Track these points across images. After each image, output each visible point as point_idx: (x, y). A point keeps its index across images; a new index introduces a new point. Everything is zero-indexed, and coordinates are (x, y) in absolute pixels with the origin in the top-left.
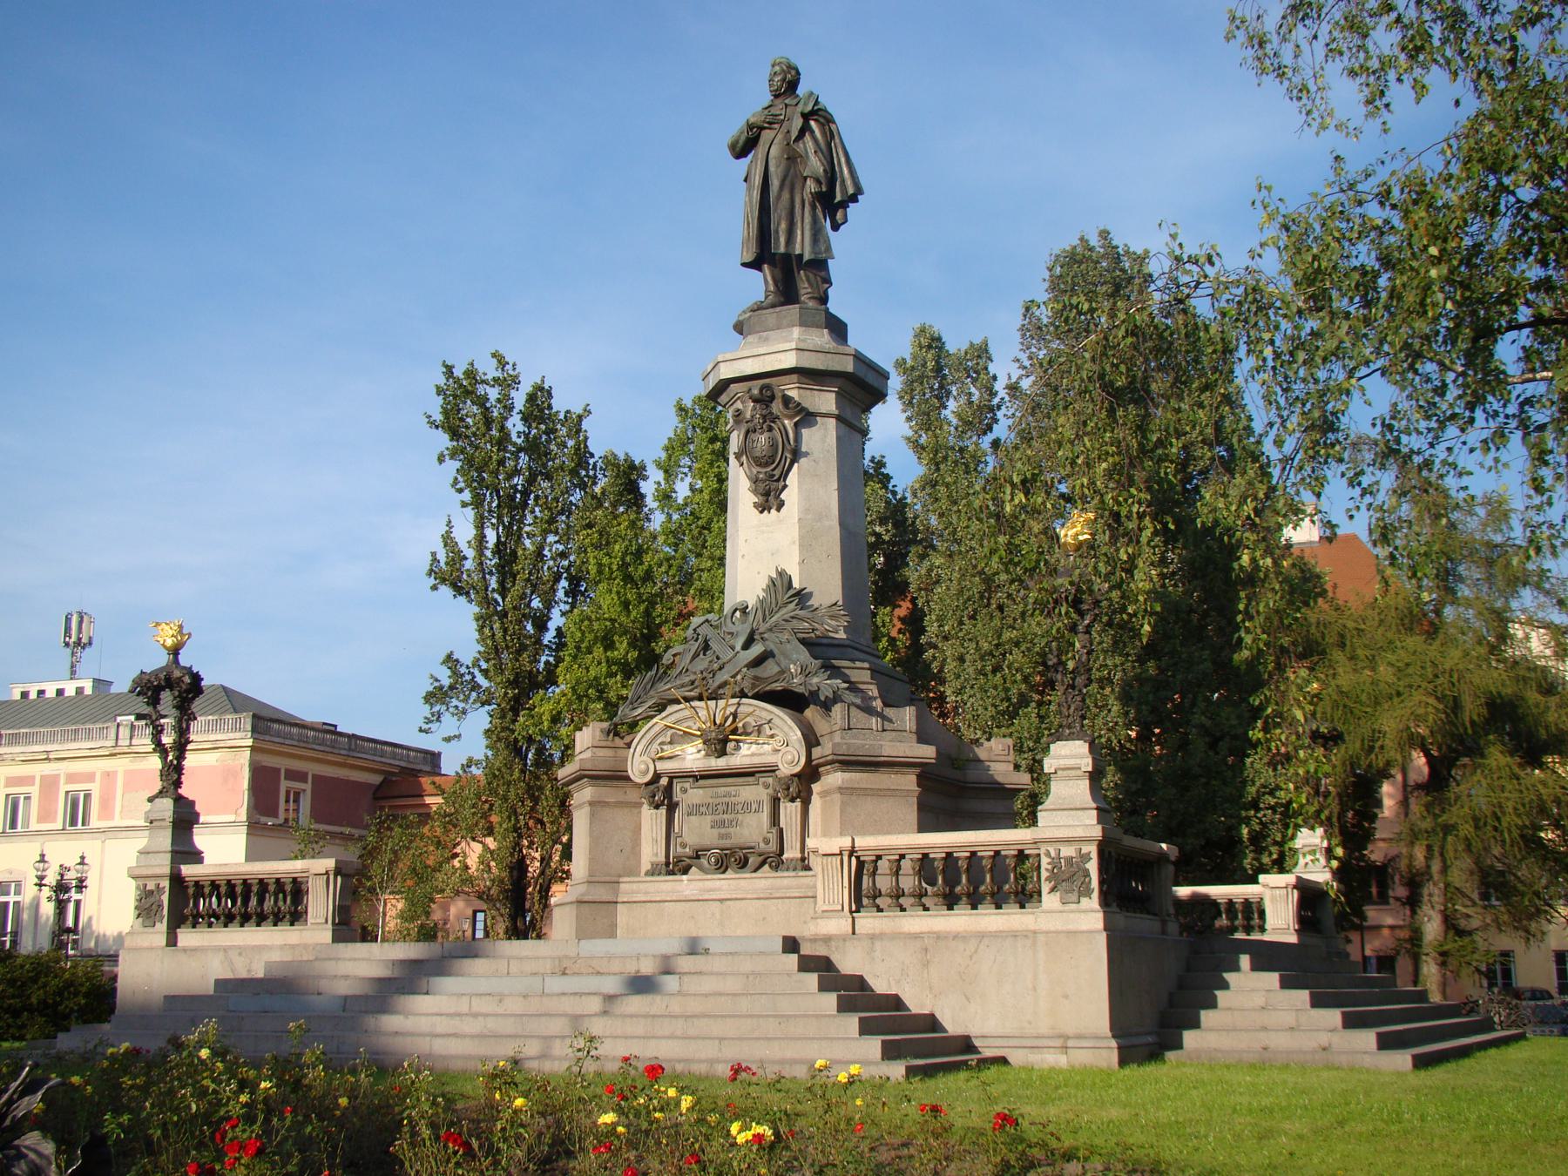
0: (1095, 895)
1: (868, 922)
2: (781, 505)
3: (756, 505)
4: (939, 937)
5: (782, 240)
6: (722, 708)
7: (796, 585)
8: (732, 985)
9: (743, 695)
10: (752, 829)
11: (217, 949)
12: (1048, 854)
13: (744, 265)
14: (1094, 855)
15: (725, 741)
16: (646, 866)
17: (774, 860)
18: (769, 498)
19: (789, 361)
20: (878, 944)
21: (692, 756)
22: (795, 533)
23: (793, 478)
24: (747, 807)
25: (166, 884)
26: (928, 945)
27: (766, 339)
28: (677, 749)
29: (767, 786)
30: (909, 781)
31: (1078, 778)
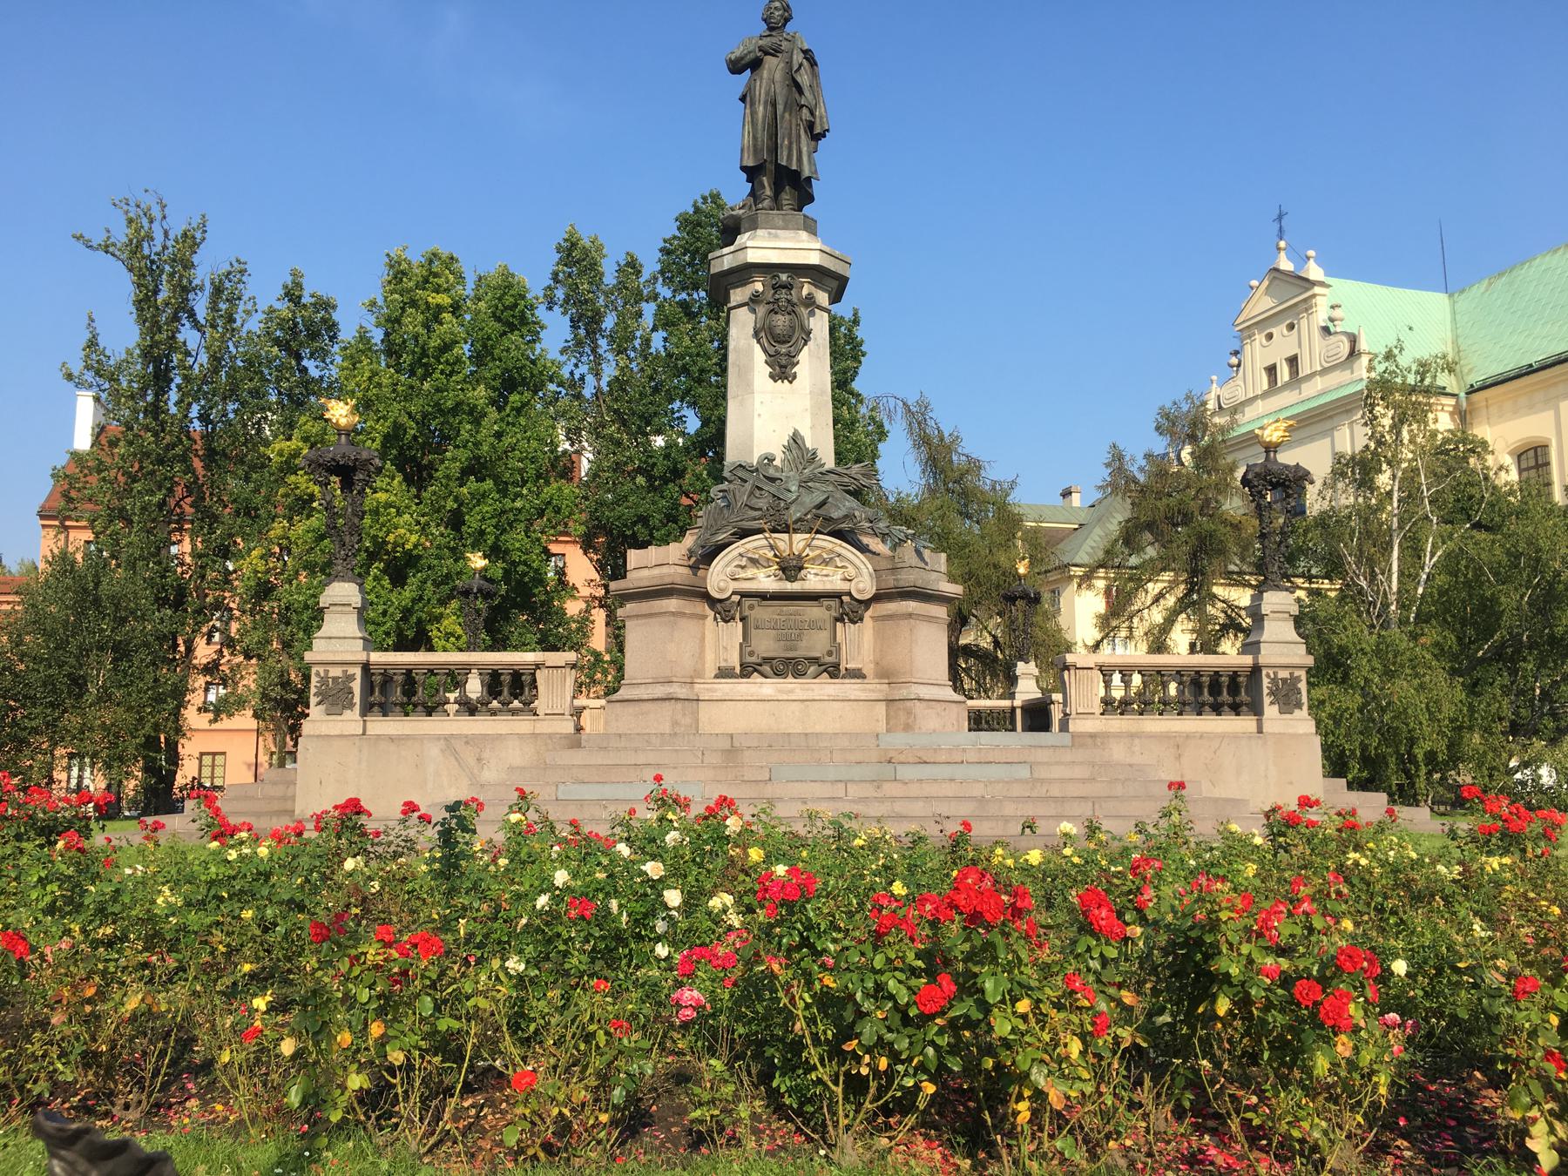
0: (1305, 707)
1: (1117, 723)
2: (791, 378)
3: (771, 376)
4: (1188, 736)
5: (785, 153)
6: (799, 540)
7: (809, 445)
8: (1079, 772)
9: (818, 532)
10: (815, 643)
11: (438, 738)
12: (1268, 676)
13: (744, 169)
14: (1304, 678)
15: (801, 568)
16: (711, 670)
17: (833, 671)
18: (782, 370)
19: (814, 259)
20: (1137, 741)
21: (766, 581)
22: (807, 403)
23: (804, 356)
24: (814, 625)
25: (357, 671)
26: (1178, 743)
27: (776, 236)
28: (750, 573)
29: (829, 608)
30: (941, 612)
31: (1285, 620)
